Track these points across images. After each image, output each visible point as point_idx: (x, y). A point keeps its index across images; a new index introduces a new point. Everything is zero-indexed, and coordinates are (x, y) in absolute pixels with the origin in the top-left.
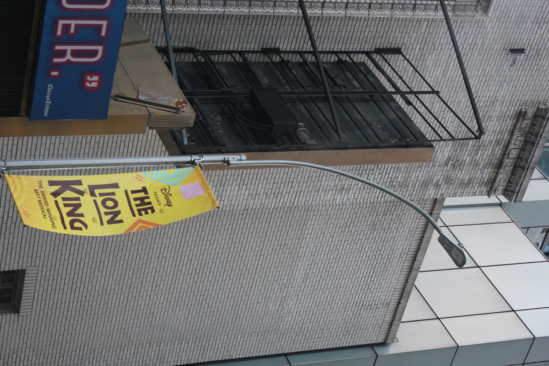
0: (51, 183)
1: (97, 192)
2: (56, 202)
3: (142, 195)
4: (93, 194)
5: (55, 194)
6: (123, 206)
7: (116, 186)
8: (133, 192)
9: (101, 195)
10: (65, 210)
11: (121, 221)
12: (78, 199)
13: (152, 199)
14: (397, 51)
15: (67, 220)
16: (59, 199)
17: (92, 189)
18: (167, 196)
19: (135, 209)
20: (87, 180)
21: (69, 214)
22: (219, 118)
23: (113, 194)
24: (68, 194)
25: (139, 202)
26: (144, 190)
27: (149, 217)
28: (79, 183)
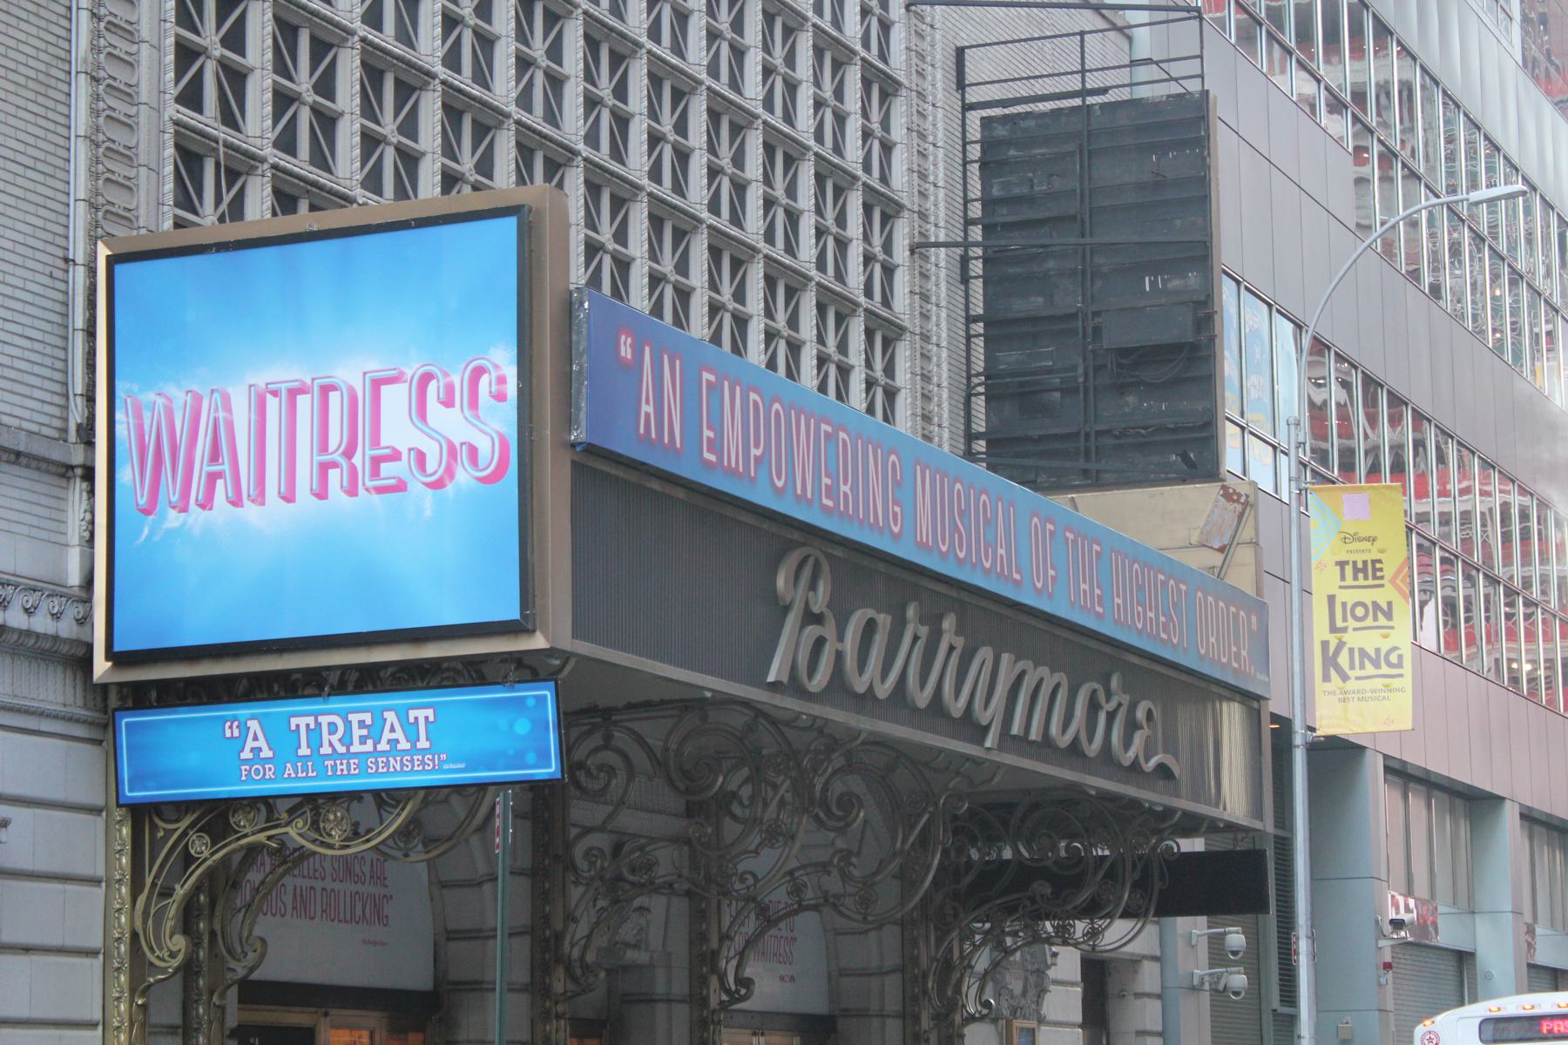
0: (1326, 678)
1: (1339, 624)
2: (1358, 678)
3: (1349, 570)
4: (1344, 630)
5: (1345, 678)
6: (1368, 596)
7: (1331, 599)
8: (1343, 578)
9: (1345, 619)
10: (1370, 669)
11: (1390, 604)
12: (1351, 650)
13: (1360, 558)
14: (960, 53)
15: (1385, 670)
16: (1351, 674)
17: (1334, 629)
18: (1356, 538)
19: (1371, 582)
20: (1320, 631)
21: (1377, 666)
22: (1131, 399)
23: (1344, 604)
24: (1343, 659)
25: (1361, 575)
26: (1342, 564)
27: (1389, 570)
28: (1325, 644)
